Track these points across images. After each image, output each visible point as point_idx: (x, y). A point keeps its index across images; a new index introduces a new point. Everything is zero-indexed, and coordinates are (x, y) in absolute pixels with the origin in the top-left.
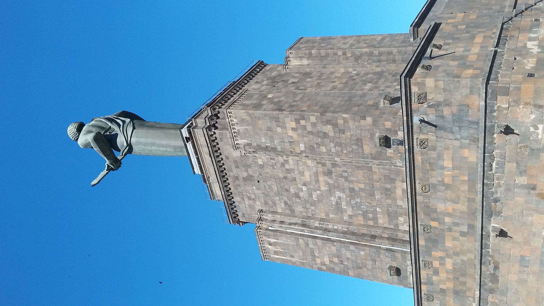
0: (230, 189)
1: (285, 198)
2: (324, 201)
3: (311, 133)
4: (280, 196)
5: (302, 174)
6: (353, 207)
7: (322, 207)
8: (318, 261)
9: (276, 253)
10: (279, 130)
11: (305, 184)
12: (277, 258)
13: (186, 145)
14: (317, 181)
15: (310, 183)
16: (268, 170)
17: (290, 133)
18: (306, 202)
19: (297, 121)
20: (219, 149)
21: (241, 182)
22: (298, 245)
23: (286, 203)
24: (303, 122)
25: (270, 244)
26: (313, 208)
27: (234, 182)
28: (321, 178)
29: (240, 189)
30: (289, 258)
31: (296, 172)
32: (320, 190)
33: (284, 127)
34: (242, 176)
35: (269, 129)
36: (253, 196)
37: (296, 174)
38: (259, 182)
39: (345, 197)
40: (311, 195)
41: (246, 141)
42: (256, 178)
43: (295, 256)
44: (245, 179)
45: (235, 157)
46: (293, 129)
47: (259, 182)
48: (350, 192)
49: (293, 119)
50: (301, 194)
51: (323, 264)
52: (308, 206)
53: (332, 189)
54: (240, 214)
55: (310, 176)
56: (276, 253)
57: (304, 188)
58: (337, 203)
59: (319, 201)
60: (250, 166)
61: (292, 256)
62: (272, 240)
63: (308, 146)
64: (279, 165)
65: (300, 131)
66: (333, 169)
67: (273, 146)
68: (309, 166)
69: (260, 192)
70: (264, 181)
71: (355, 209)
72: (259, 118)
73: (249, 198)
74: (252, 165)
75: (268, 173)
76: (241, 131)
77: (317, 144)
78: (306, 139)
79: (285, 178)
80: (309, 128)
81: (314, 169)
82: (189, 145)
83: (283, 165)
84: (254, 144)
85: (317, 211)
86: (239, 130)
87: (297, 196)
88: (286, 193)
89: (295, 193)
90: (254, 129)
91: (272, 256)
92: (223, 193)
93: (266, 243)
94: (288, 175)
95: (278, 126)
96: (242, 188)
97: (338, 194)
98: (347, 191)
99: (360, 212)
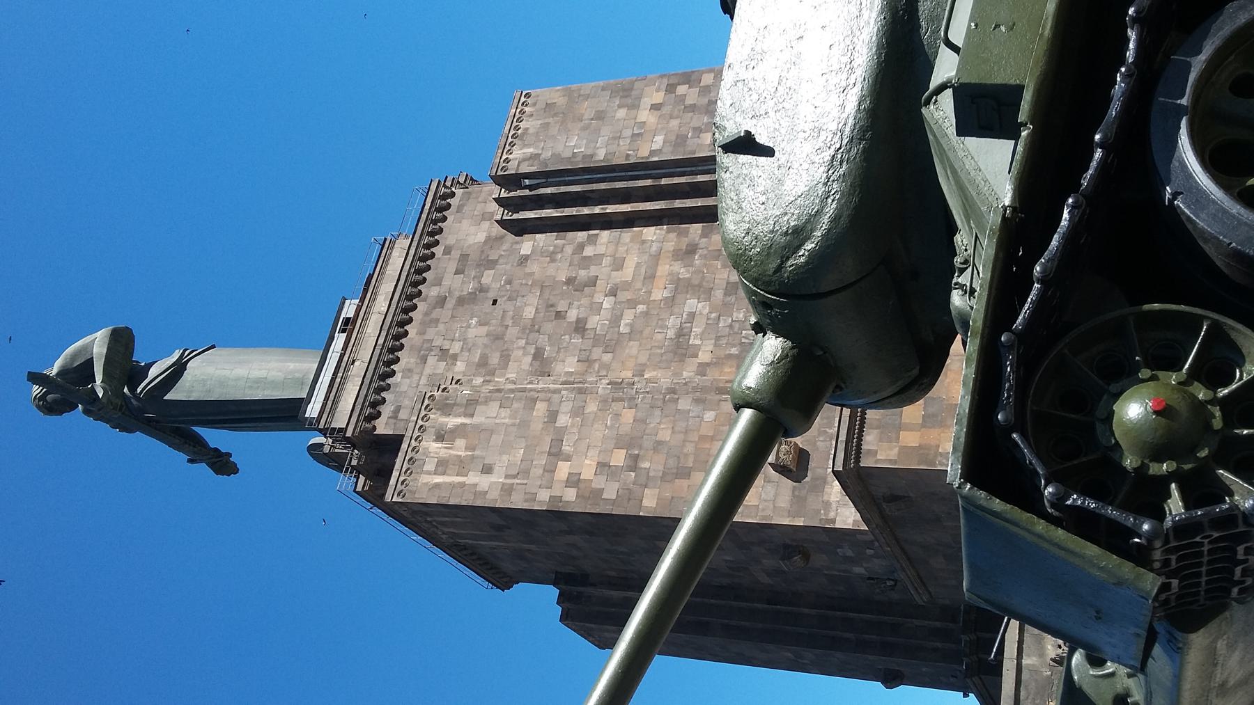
0: (406, 333)
1: (543, 340)
2: (647, 332)
3: (693, 108)
4: (533, 336)
5: (618, 265)
6: (718, 338)
7: (634, 351)
8: (563, 470)
9: (443, 466)
10: (622, 113)
11: (613, 293)
12: (437, 486)
13: (331, 338)
14: (651, 277)
15: (627, 286)
16: (533, 267)
17: (644, 115)
18: (597, 340)
19: (671, 89)
20: (441, 231)
21: (445, 313)
22: (524, 424)
23: (538, 355)
24: (682, 89)
25: (440, 437)
26: (607, 357)
27: (426, 314)
28: (664, 269)
29: (431, 333)
30: (473, 478)
31: (606, 261)
32: (647, 302)
33: (635, 106)
34: (457, 294)
35: (600, 116)
36: (456, 347)
37: (602, 271)
38: (495, 302)
39: (707, 311)
40: (616, 320)
41: (531, 150)
42: (492, 295)
43: (496, 469)
44: (461, 301)
45: (470, 246)
46: (655, 107)
47: (495, 302)
48: (725, 294)
49: (664, 87)
50: (593, 322)
51: (573, 480)
52: (597, 353)
53: (681, 287)
54: (386, 410)
55: (638, 265)
56: (443, 466)
57: (607, 303)
58: (681, 328)
59: (633, 333)
60: (491, 264)
61: (487, 470)
62: (452, 421)
63: (673, 138)
64: (569, 250)
65: (666, 110)
66: (704, 240)
67: (589, 152)
68: (644, 242)
69: (484, 330)
70: (510, 299)
71: (724, 341)
72: (587, 97)
73: (444, 354)
74: (501, 261)
75: (532, 274)
76: (531, 131)
77: (695, 129)
78: (674, 123)
79: (570, 281)
80: (689, 101)
81: (654, 248)
82: (340, 339)
83: (581, 247)
84: (547, 154)
85: (614, 365)
86: (527, 129)
87: (580, 327)
88: (549, 327)
89: (578, 321)
90: (563, 122)
91: (425, 479)
92: (381, 341)
93: (431, 433)
94: (583, 273)
95: (620, 107)
96: (441, 327)
97: (692, 304)
98: (719, 294)
99: (734, 351)
